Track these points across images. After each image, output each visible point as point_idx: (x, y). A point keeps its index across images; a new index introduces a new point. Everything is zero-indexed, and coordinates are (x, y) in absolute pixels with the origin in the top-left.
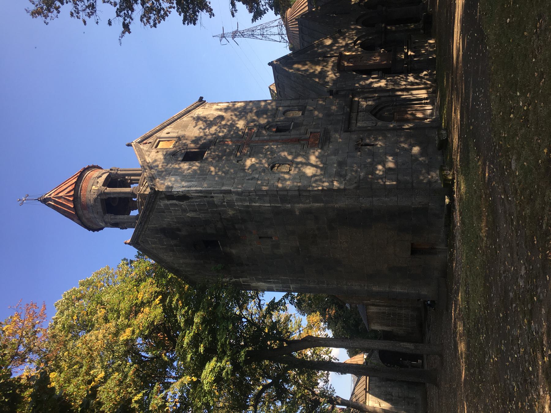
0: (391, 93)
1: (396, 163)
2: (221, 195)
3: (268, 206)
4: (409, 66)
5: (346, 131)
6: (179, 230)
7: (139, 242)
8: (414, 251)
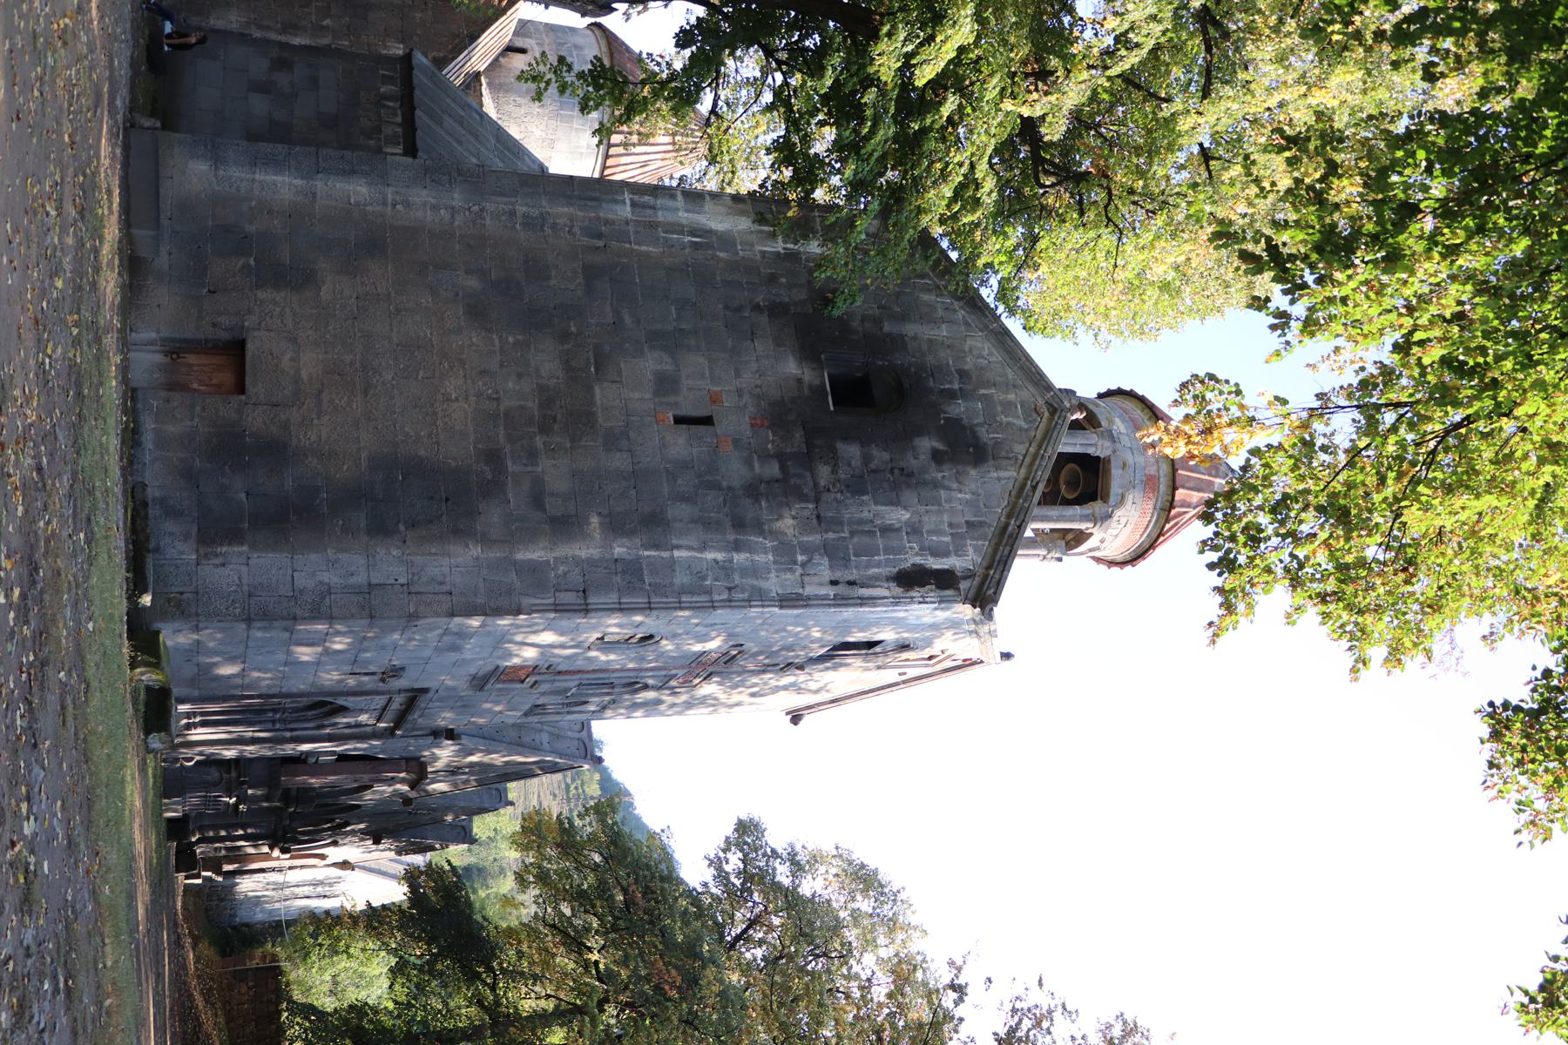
0: (288, 734)
1: (289, 653)
2: (809, 590)
3: (678, 547)
4: (233, 774)
5: (425, 691)
6: (937, 457)
7: (1047, 414)
8: (236, 349)
